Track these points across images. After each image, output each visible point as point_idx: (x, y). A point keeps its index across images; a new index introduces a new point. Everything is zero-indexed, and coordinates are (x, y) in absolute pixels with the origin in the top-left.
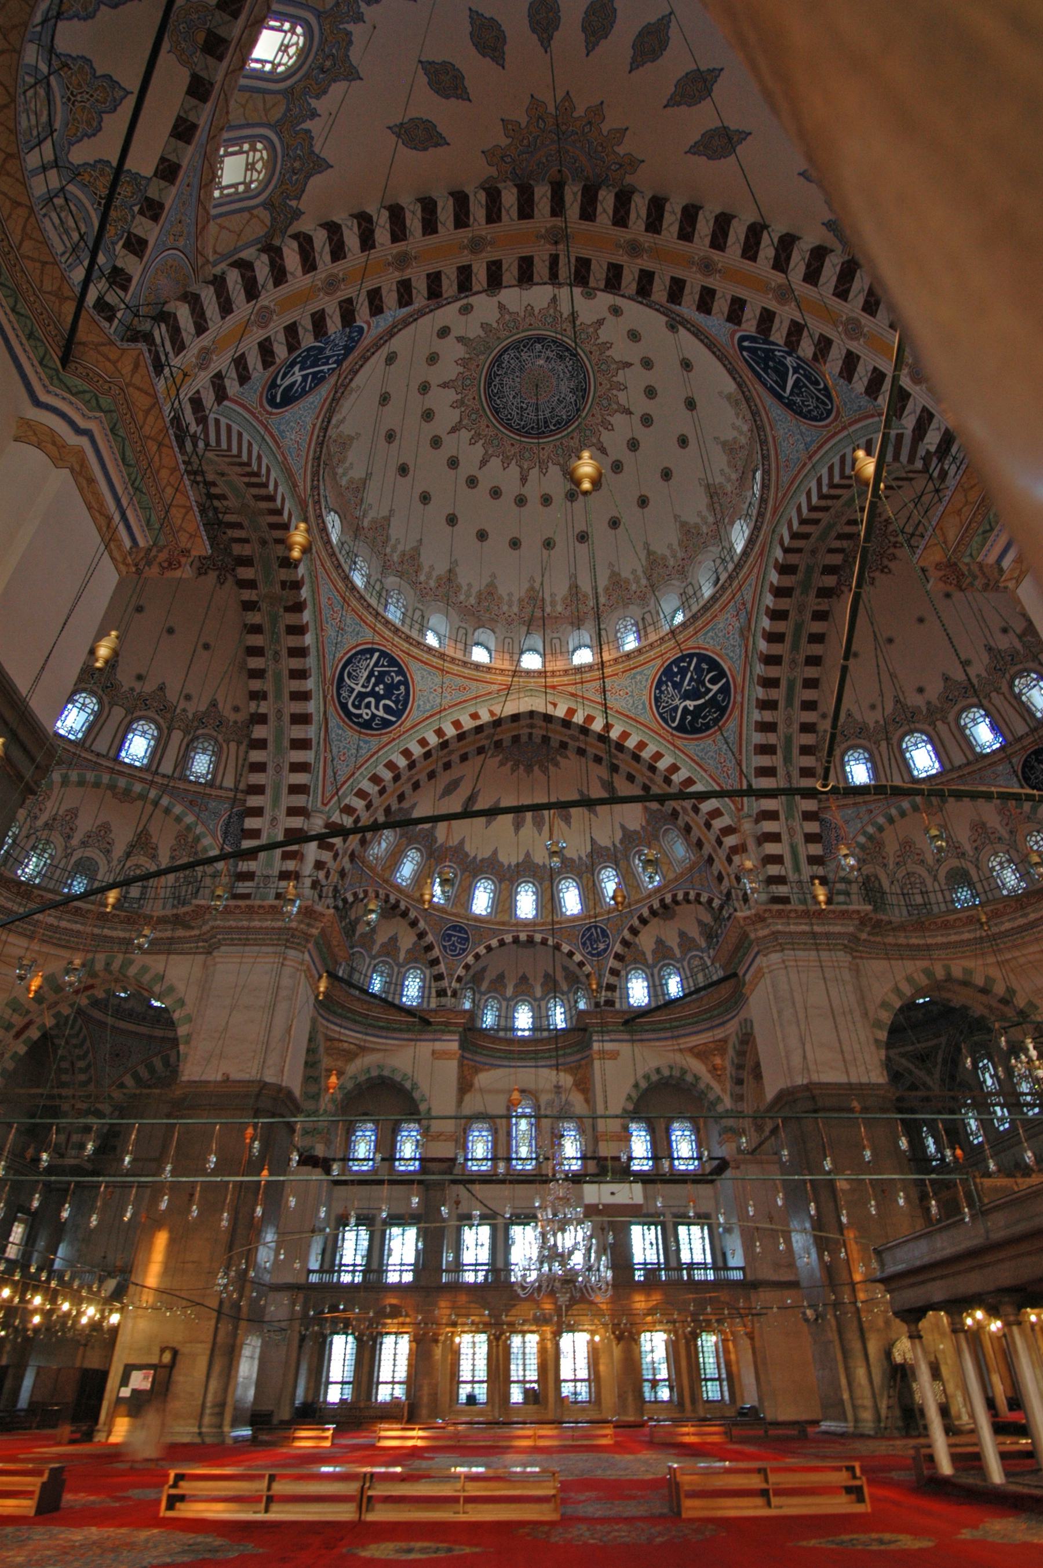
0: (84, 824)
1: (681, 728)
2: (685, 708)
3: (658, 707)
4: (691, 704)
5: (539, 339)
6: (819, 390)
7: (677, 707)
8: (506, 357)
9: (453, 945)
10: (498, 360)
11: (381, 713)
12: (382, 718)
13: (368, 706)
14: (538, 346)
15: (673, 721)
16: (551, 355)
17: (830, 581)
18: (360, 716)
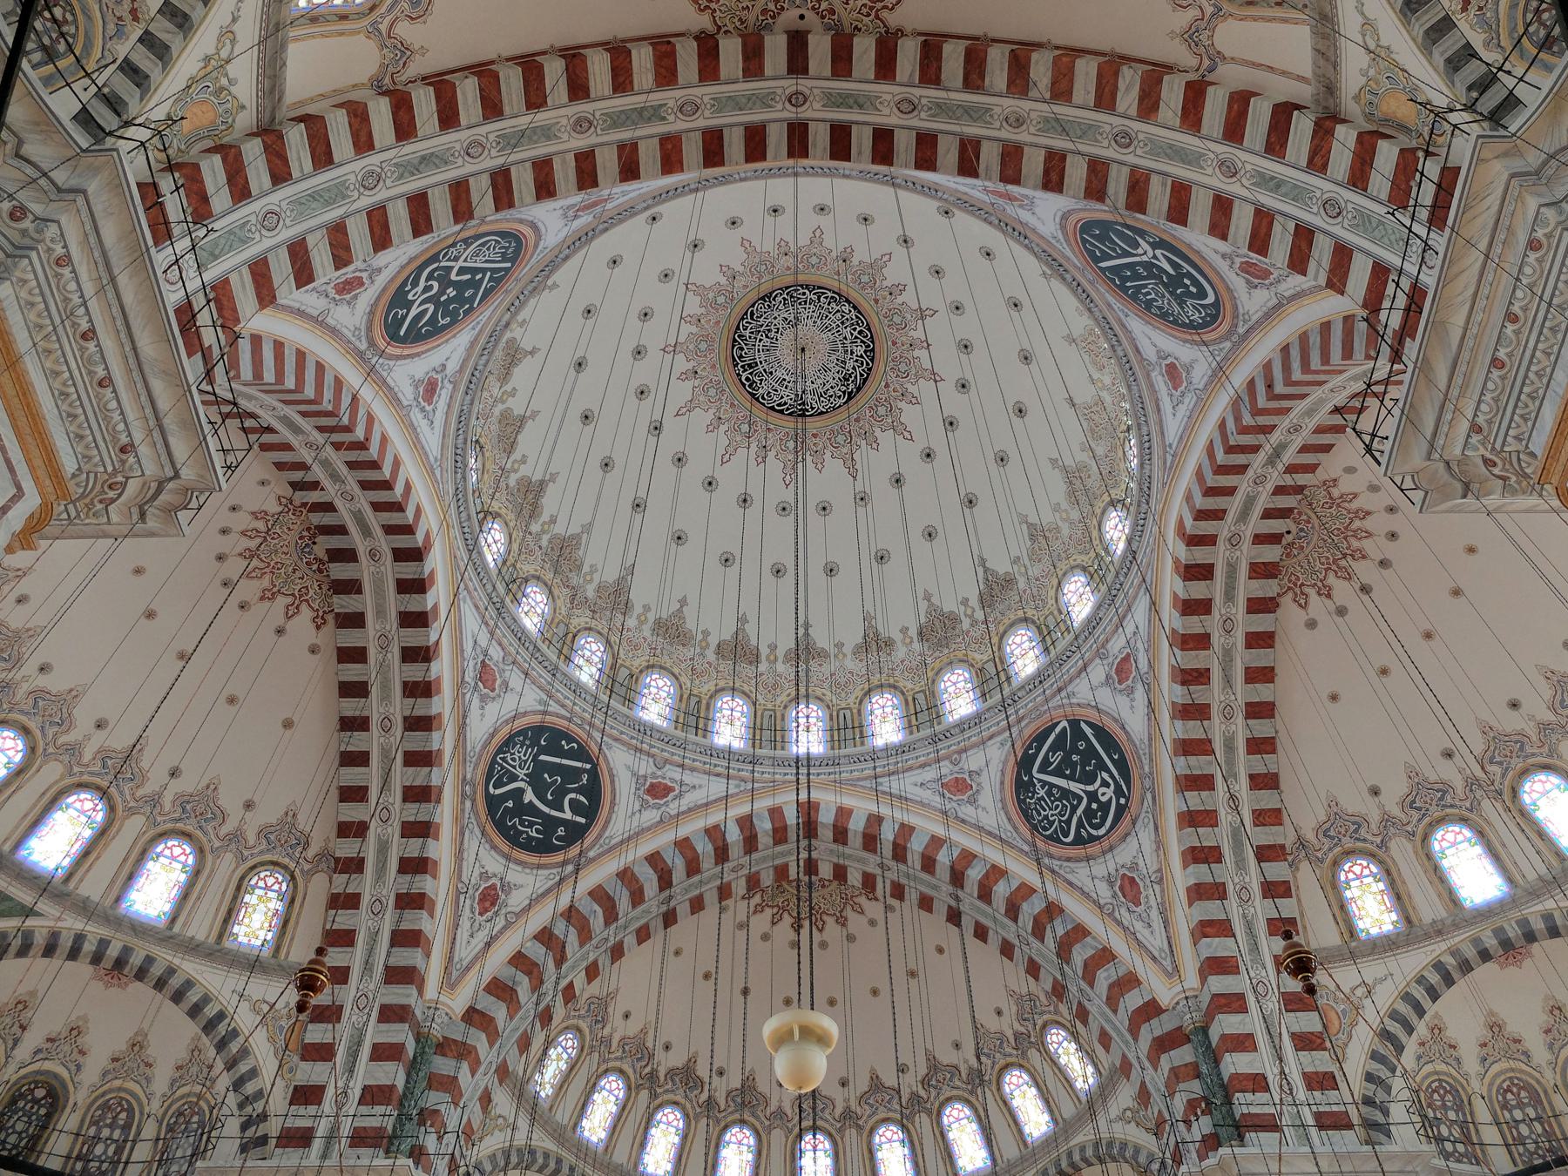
1: (492, 803)
2: (521, 791)
3: (500, 751)
4: (529, 796)
5: (871, 352)
6: (1080, 825)
7: (514, 778)
8: (846, 308)
10: (840, 297)
13: (427, 289)
14: (860, 350)
15: (495, 787)
16: (850, 365)
18: (415, 284)
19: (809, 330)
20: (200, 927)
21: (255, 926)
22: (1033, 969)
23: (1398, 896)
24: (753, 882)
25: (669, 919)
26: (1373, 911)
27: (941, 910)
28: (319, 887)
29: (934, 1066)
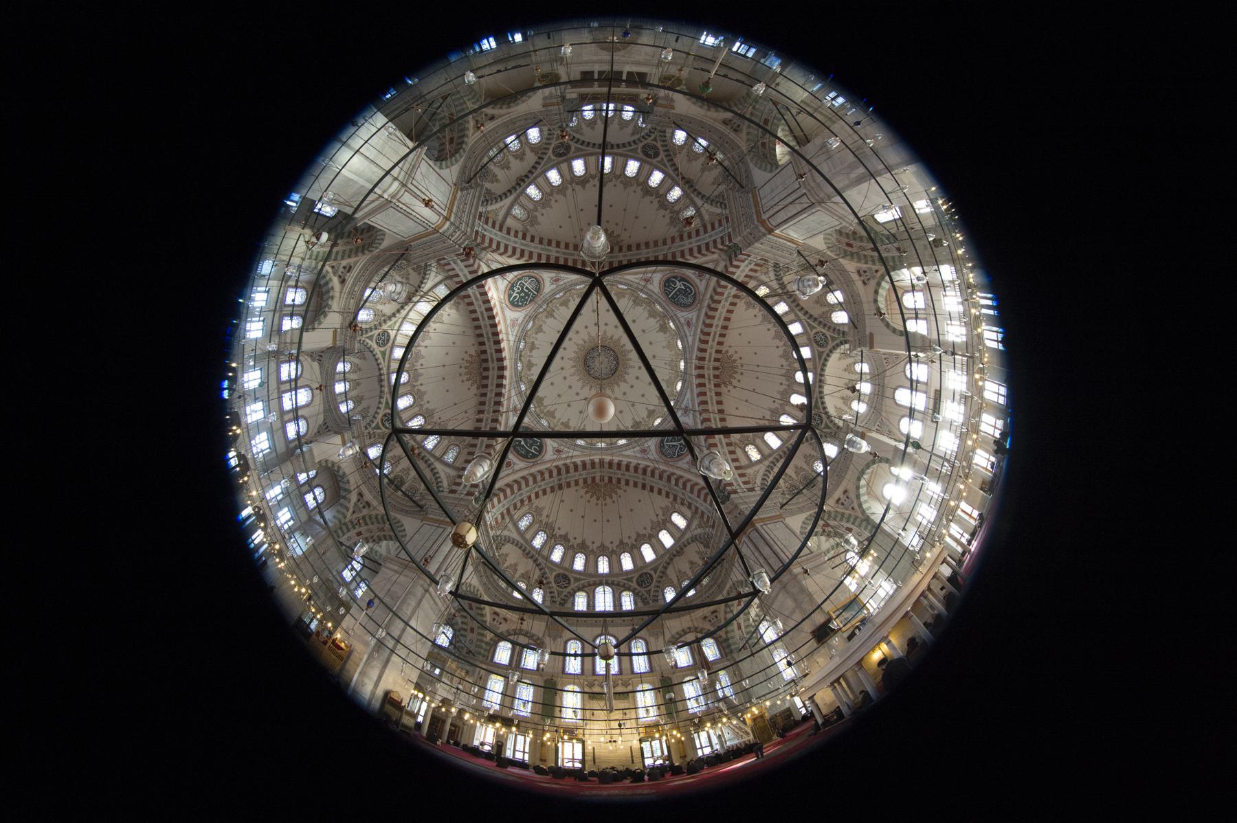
17: (589, 481)
19: (602, 358)
20: (438, 454)
21: (450, 457)
22: (667, 496)
23: (760, 451)
24: (585, 481)
25: (560, 487)
26: (754, 455)
27: (640, 485)
28: (466, 451)
29: (638, 535)
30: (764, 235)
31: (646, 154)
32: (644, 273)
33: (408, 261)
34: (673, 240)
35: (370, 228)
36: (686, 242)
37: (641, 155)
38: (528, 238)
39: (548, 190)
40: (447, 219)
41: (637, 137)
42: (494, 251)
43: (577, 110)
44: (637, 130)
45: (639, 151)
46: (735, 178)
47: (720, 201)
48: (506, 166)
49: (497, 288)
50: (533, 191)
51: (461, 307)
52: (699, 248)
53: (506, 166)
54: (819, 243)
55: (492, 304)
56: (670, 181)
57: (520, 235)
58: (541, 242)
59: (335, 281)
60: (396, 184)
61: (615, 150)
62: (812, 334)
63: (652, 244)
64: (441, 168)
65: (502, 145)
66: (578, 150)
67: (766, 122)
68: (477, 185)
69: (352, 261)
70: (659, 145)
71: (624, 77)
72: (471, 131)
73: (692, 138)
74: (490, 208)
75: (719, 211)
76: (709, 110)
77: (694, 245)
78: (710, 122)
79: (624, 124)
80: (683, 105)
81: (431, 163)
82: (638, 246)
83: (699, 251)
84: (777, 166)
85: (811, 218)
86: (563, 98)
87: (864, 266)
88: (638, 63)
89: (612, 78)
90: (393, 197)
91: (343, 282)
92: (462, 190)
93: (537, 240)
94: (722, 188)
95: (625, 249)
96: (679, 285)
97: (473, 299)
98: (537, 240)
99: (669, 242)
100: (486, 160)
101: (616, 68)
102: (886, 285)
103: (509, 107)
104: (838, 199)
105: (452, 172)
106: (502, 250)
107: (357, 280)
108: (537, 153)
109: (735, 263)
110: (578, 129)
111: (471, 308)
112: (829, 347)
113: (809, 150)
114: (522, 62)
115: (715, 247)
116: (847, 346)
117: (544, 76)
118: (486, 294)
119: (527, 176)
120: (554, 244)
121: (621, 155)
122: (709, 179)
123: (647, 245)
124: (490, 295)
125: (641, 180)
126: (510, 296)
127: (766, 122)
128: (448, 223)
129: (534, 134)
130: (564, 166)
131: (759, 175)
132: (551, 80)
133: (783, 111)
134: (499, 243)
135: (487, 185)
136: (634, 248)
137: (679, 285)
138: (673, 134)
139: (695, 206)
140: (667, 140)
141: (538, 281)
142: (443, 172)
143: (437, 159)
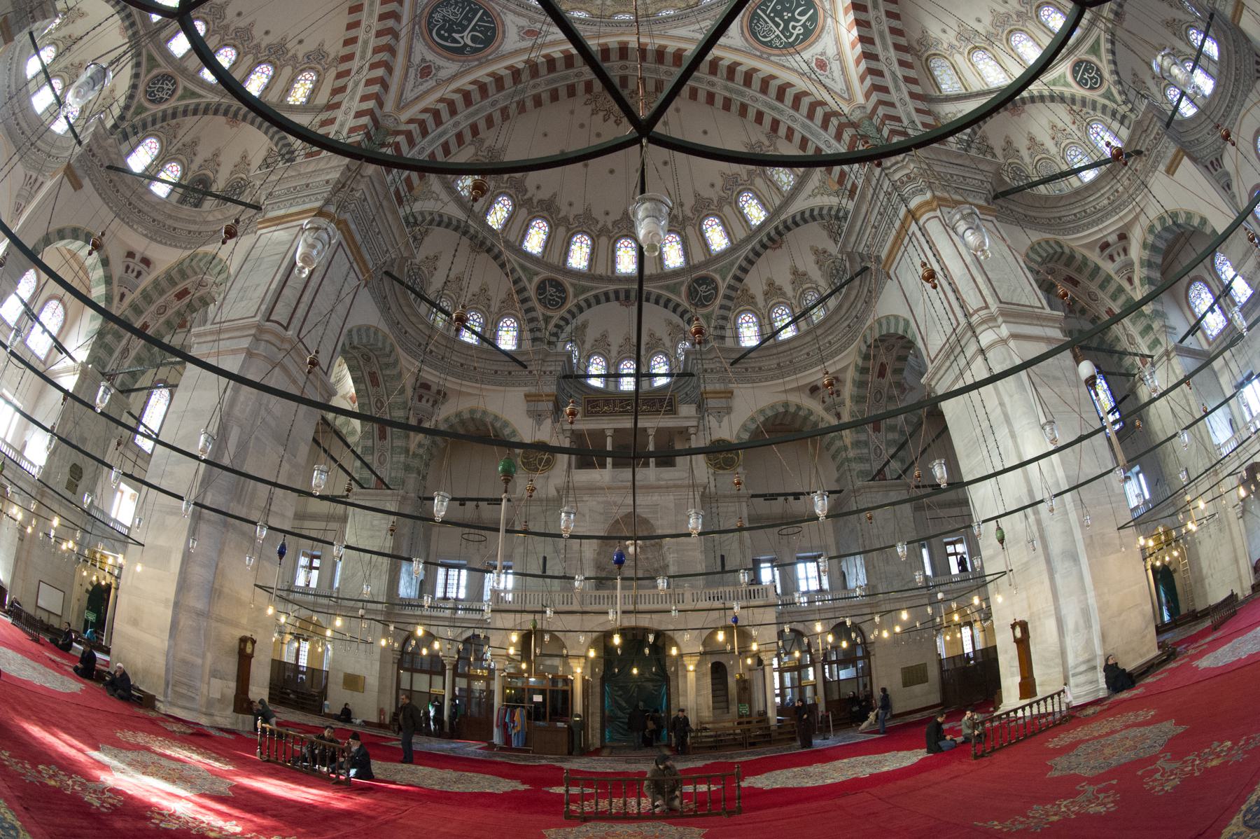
0: (783, 279)
9: (1091, 79)
11: (804, 19)
12: (808, 20)
13: (794, 27)
30: (328, 202)
31: (559, 286)
32: (542, 46)
33: (998, 174)
34: (490, 121)
35: (1047, 288)
36: (464, 125)
37: (567, 282)
38: (767, 121)
39: (727, 209)
40: (912, 215)
41: (581, 318)
42: (836, 114)
43: (681, 376)
44: (578, 337)
45: (571, 290)
46: (399, 284)
47: (418, 226)
48: (799, 276)
49: (838, 41)
50: (755, 214)
51: (916, 35)
52: (438, 121)
53: (799, 276)
54: (232, 253)
55: (851, 16)
56: (512, 238)
57: (782, 131)
58: (744, 109)
59: (1137, 237)
60: (986, 338)
61: (612, 287)
62: (182, 83)
63: (529, 104)
64: (907, 322)
65: (803, 324)
66: (674, 289)
67: (383, 436)
68: (850, 256)
69: (1095, 257)
70: (540, 311)
71: (609, 460)
72: (850, 375)
73: (489, 339)
74: (834, 201)
75: (417, 207)
76: (472, 411)
77: (448, 122)
78: (467, 386)
79: (601, 346)
80: (511, 409)
81: (920, 344)
82: (554, 96)
83: (436, 114)
84: (344, 352)
85: (260, 292)
86: (701, 407)
87: (146, 281)
88: (592, 489)
89: (630, 453)
90: (992, 318)
91: (1123, 237)
92: (878, 258)
93: (751, 114)
94: (420, 256)
95: (581, 88)
96: (466, 38)
97: (889, 40)
98: (751, 114)
99: (497, 117)
100: (832, 303)
101: (626, 474)
102: (97, 292)
103: (786, 405)
104: (232, 364)
105: (889, 304)
106: (819, 112)
107: (1101, 215)
108: (745, 291)
109: (365, 120)
110: (677, 333)
111: (895, 24)
112: (141, 88)
113: (306, 422)
114: (763, 507)
115: (409, 135)
116: (109, 123)
117: (728, 464)
118: (862, 39)
119: (764, 247)
120: (719, 102)
121: (601, 278)
122: (443, 259)
123: (538, 102)
124: (855, 32)
125: (562, 230)
126: (813, 19)
127: (383, 436)
128: (913, 204)
129: (749, 336)
130: (699, 257)
131: (367, 313)
132: (720, 453)
133: (366, 473)
134: (825, 126)
135: (833, 249)
136: (563, 93)
137: (466, 38)
138: (520, 340)
139: (458, 200)
140: (530, 329)
141: (754, 34)
142: (904, 312)
143: (910, 344)
